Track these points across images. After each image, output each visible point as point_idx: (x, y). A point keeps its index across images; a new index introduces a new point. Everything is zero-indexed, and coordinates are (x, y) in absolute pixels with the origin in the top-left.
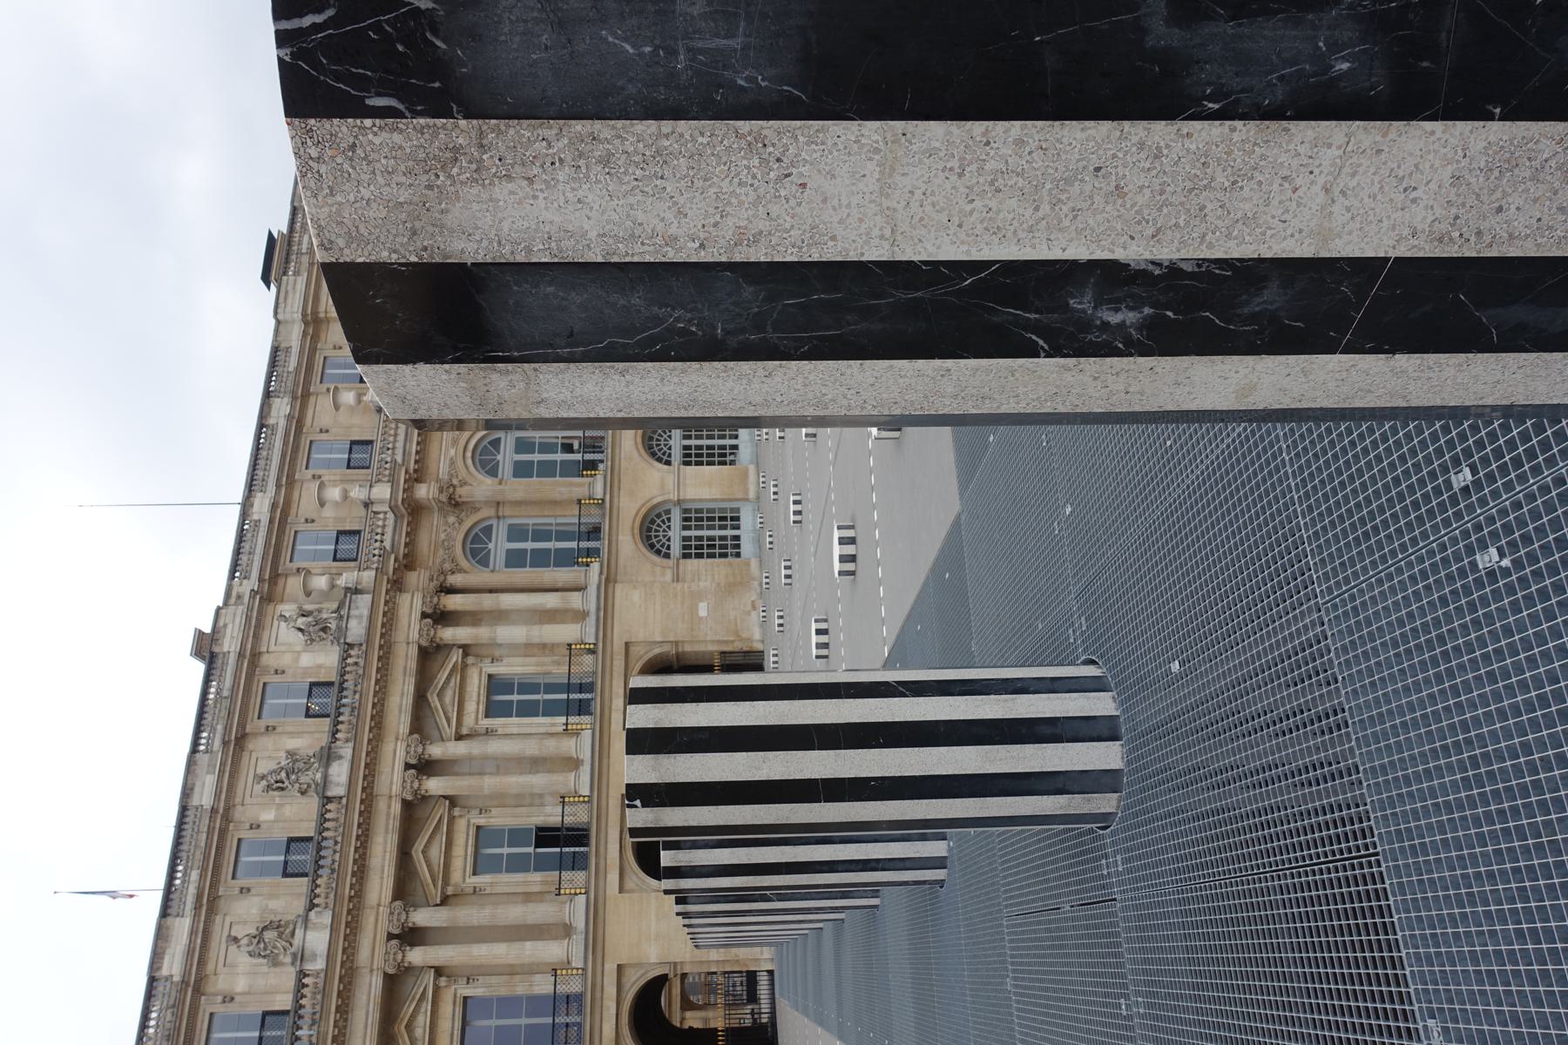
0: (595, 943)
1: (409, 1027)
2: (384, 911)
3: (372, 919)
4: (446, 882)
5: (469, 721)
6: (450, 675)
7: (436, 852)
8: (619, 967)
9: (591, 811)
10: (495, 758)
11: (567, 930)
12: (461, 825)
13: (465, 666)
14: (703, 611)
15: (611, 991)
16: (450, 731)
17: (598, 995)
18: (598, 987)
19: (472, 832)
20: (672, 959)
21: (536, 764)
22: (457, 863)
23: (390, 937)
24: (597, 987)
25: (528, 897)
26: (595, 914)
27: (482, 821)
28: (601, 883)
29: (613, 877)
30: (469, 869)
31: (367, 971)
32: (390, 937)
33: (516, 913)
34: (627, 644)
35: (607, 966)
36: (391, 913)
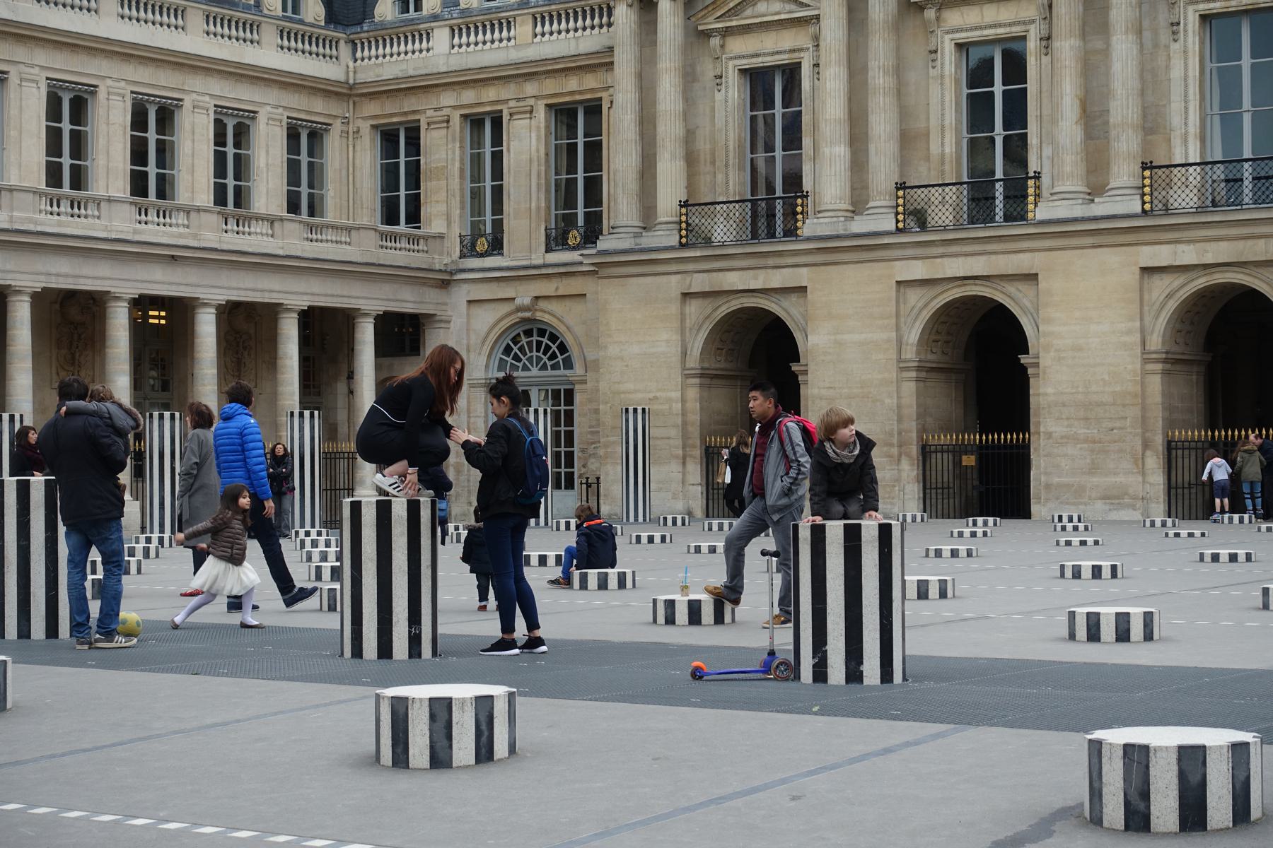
0: (835, 250)
8: (802, 290)
9: (945, 229)
10: (1106, 52)
11: (858, 206)
15: (776, 279)
17: (771, 262)
18: (779, 261)
19: (1016, 30)
20: (811, 368)
24: (775, 261)
25: (909, 139)
27: (1032, 45)
28: (910, 252)
29: (918, 270)
30: (963, 37)
33: (882, 124)
35: (804, 270)
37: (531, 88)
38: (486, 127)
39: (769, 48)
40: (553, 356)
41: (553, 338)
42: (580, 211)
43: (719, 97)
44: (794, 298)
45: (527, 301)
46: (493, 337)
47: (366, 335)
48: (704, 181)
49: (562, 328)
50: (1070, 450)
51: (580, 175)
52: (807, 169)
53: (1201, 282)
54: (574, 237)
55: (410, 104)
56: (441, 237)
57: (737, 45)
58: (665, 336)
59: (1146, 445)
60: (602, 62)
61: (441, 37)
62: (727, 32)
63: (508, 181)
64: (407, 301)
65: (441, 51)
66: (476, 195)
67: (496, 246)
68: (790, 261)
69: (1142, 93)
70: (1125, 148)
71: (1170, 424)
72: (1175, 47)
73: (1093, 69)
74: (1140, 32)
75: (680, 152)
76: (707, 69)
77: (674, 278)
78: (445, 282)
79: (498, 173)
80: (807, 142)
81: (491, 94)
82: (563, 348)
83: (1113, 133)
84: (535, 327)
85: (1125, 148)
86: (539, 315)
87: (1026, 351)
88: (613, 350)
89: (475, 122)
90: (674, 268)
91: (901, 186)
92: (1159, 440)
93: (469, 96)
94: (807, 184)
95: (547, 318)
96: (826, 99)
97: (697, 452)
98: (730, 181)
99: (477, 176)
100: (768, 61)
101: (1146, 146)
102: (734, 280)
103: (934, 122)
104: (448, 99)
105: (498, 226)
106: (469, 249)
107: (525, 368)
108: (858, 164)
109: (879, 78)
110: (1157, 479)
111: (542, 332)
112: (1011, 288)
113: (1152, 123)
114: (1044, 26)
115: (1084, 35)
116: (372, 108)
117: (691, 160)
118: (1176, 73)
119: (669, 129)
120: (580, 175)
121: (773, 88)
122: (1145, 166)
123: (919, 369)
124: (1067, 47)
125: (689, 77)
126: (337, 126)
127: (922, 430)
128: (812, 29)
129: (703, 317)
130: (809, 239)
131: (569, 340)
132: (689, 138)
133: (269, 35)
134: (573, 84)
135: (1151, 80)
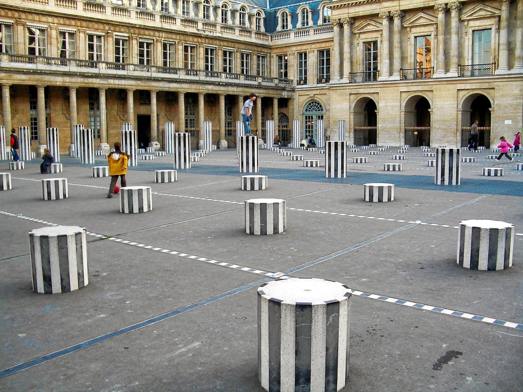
0: (386, 84)
1: (369, 24)
2: (397, 8)
3: (395, 4)
4: (411, 27)
5: (471, 23)
6: (489, 11)
7: (422, 21)
12: (432, 29)
13: (494, 17)
14: (508, 122)
15: (372, 91)
16: (464, 17)
17: (371, 86)
21: (446, 54)
22: (418, 30)
23: (389, 12)
25: (403, 59)
26: (394, 83)
29: (405, 89)
31: (381, 7)
32: (389, 12)
33: (397, 55)
34: (494, 88)
36: (397, 11)
37: (313, 46)
38: (303, 56)
39: (370, 37)
40: (318, 108)
41: (318, 104)
42: (325, 75)
43: (358, 48)
44: (376, 95)
45: (313, 95)
46: (304, 104)
47: (276, 102)
48: (355, 67)
49: (321, 102)
50: (440, 131)
51: (325, 66)
52: (379, 65)
53: (471, 93)
54: (324, 81)
55: (285, 50)
56: (292, 81)
57: (362, 36)
58: (345, 103)
59: (457, 130)
60: (331, 40)
61: (292, 35)
62: (360, 33)
63: (308, 67)
64: (285, 95)
65: (292, 38)
66: (301, 71)
67: (305, 83)
68: (375, 86)
69: (458, 48)
70: (454, 60)
71: (462, 125)
72: (466, 38)
73: (446, 42)
74: (458, 34)
75: (349, 61)
76: (355, 42)
77: (348, 90)
78: (293, 90)
79: (305, 66)
80: (379, 59)
81: (304, 47)
82: (321, 106)
83: (451, 58)
84: (314, 101)
85: (454, 60)
86: (315, 99)
87: (491, 107)
88: (333, 107)
89: (301, 54)
90: (348, 88)
91: (401, 69)
92: (460, 128)
93: (299, 48)
94: (379, 69)
95: (317, 99)
96: (383, 49)
97: (353, 130)
98: (360, 68)
99: (301, 66)
100: (370, 40)
101: (459, 61)
102: (362, 91)
103: (409, 55)
104: (294, 49)
105: (306, 78)
106: (299, 83)
107: (312, 111)
108: (391, 64)
109: (396, 44)
110: (459, 138)
111: (316, 102)
112: (427, 93)
113: (460, 56)
114: (436, 33)
115: (445, 35)
116: (277, 51)
117: (352, 63)
118: (466, 44)
119: (346, 56)
120: (325, 66)
121: (371, 47)
122: (459, 65)
123: (462, 111)
124: (441, 37)
125: (351, 44)
126: (268, 55)
127: (405, 126)
128: (380, 33)
129: (354, 99)
130: (380, 81)
131: (322, 105)
132: (351, 58)
133: (253, 35)
134: (323, 45)
135: (460, 45)
